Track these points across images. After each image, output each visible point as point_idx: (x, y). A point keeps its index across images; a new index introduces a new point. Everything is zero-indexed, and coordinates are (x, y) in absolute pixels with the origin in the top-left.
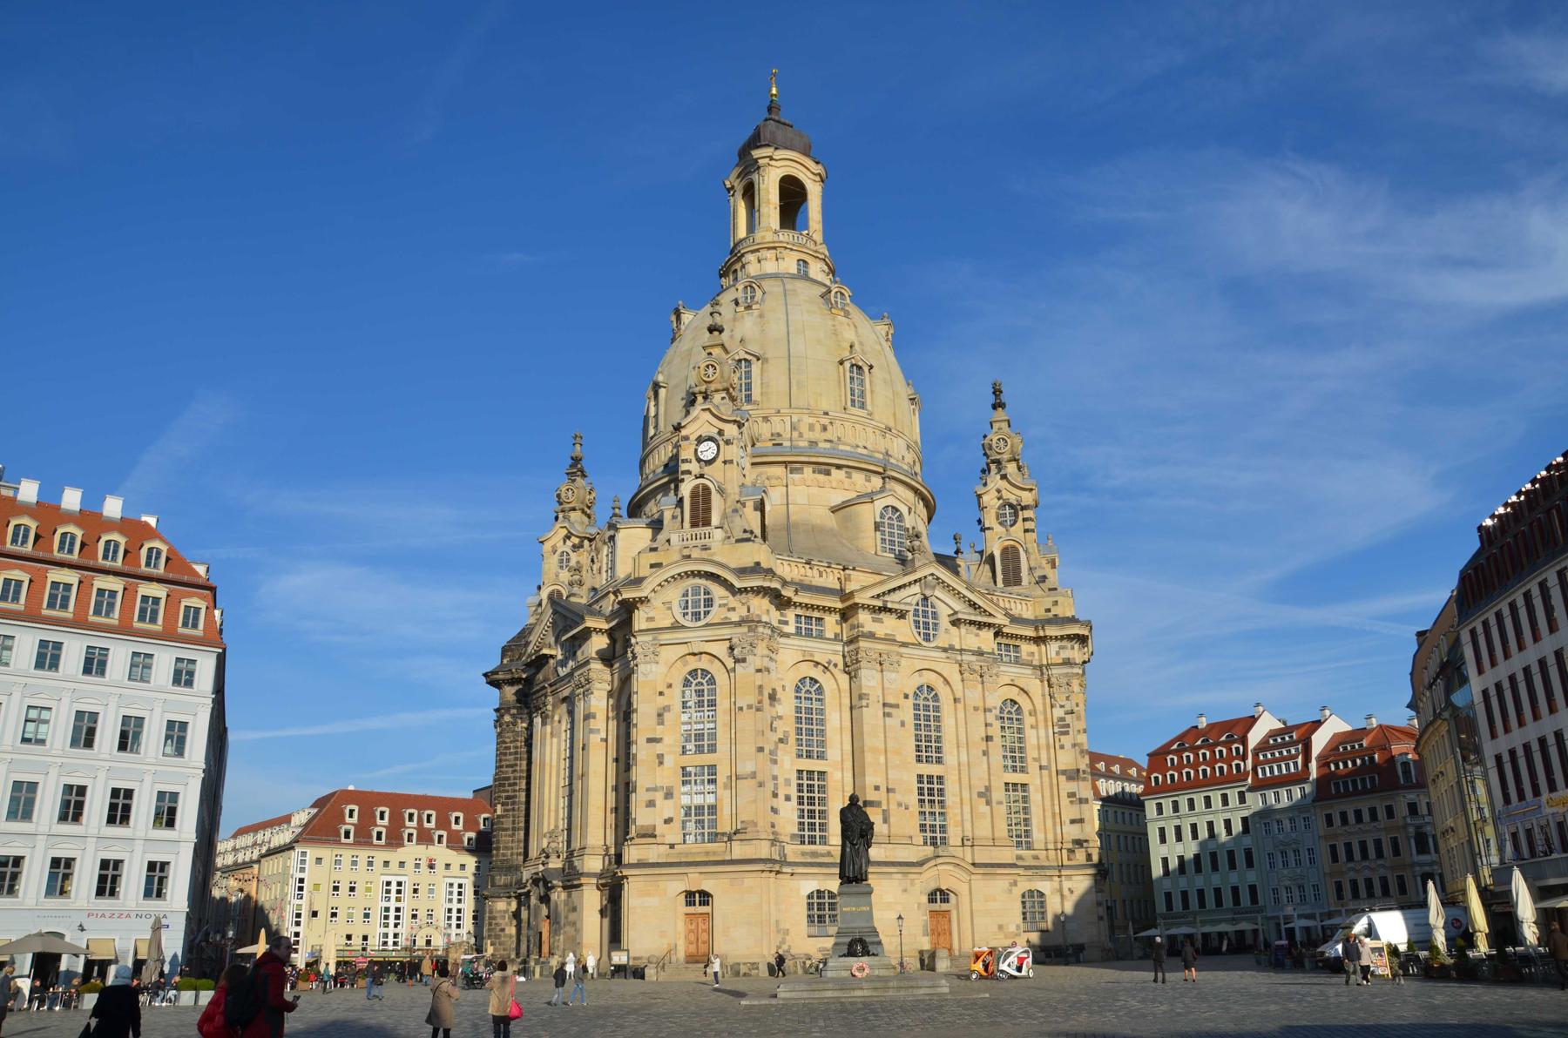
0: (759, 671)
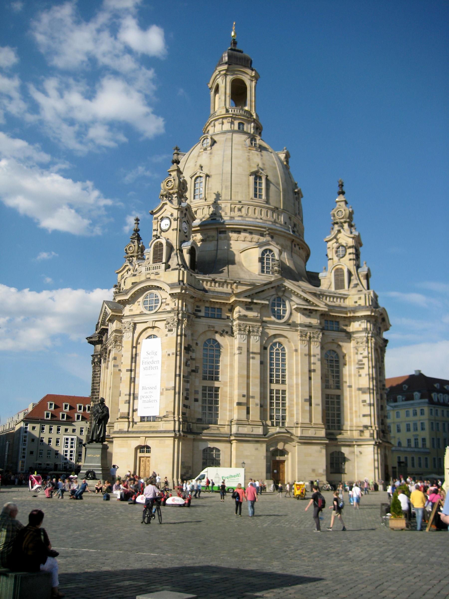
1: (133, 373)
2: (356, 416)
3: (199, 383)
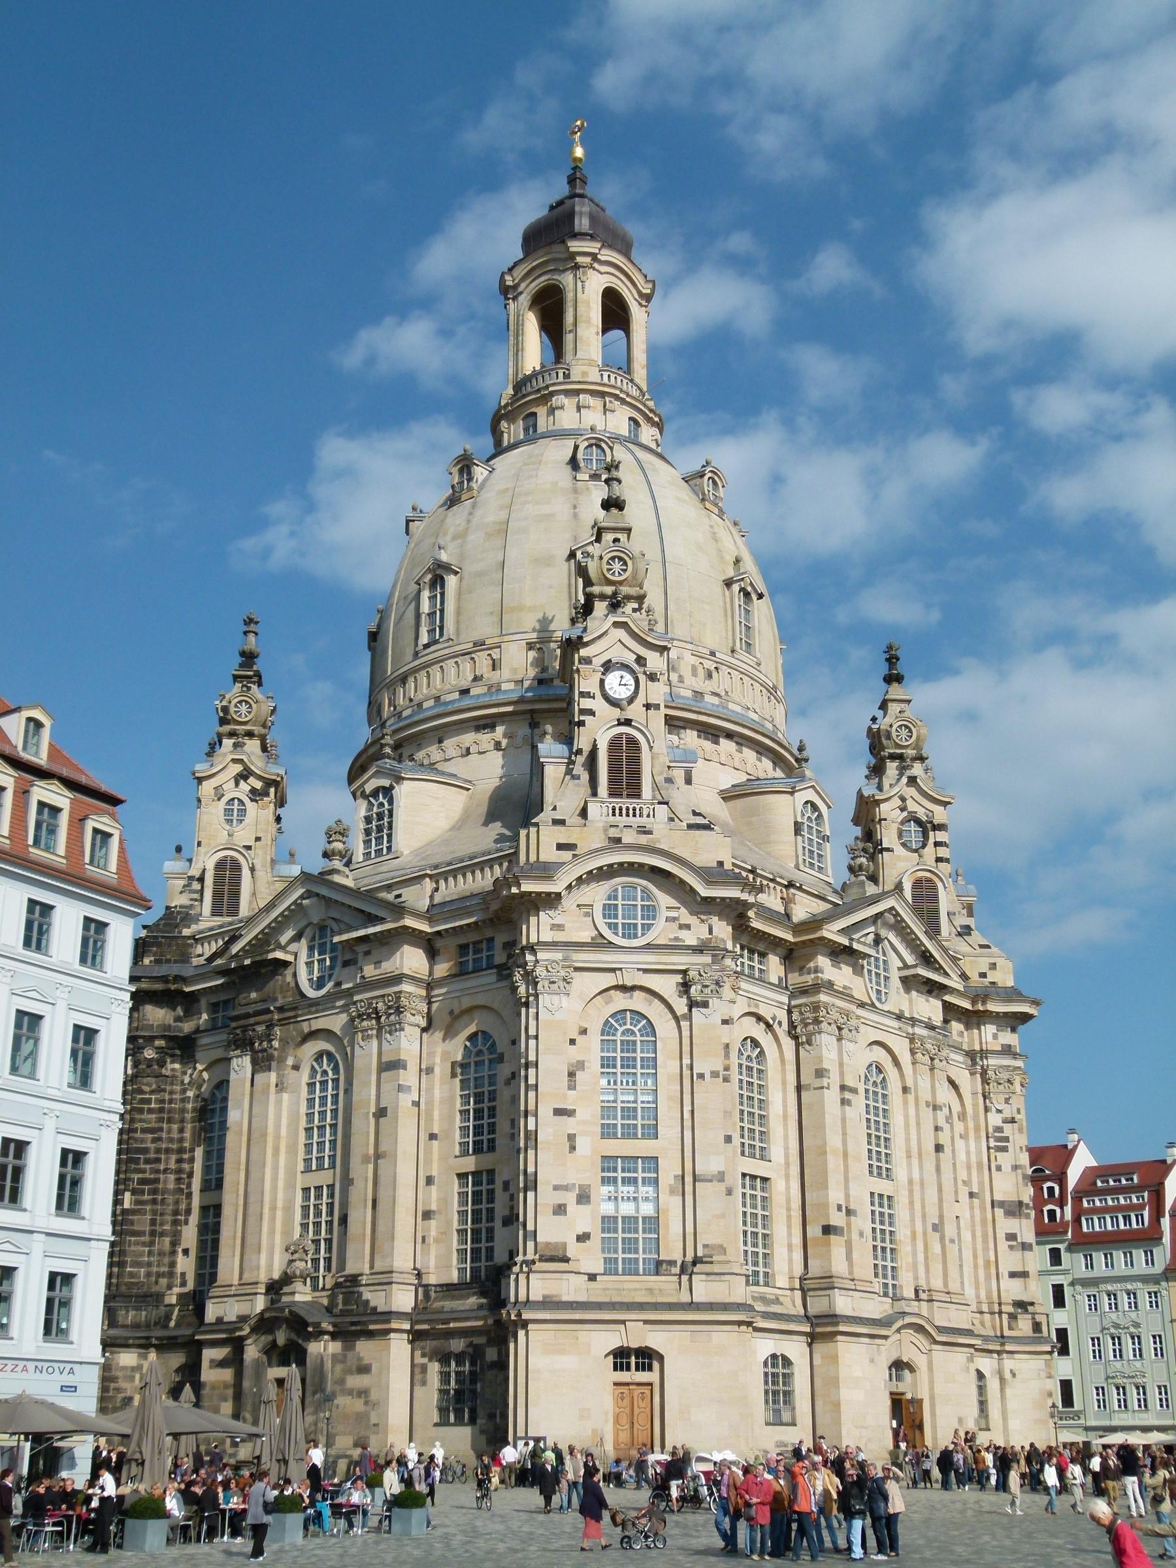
0: (725, 1022)
1: (571, 1119)
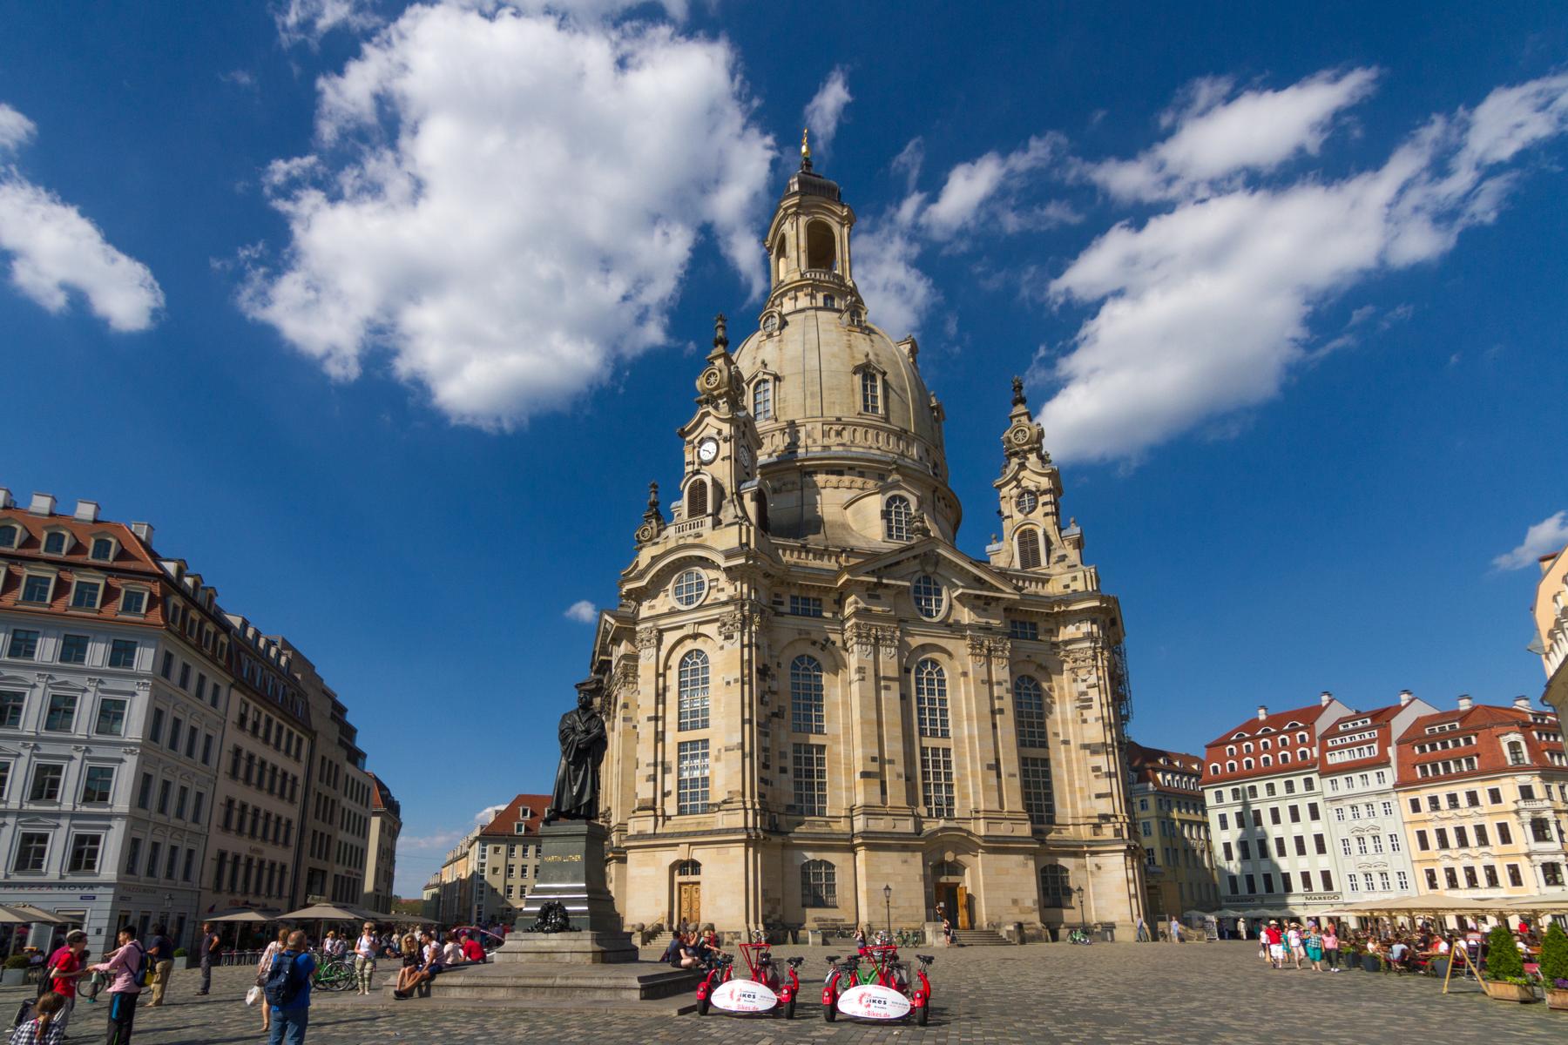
2: (1083, 798)
3: (785, 737)
